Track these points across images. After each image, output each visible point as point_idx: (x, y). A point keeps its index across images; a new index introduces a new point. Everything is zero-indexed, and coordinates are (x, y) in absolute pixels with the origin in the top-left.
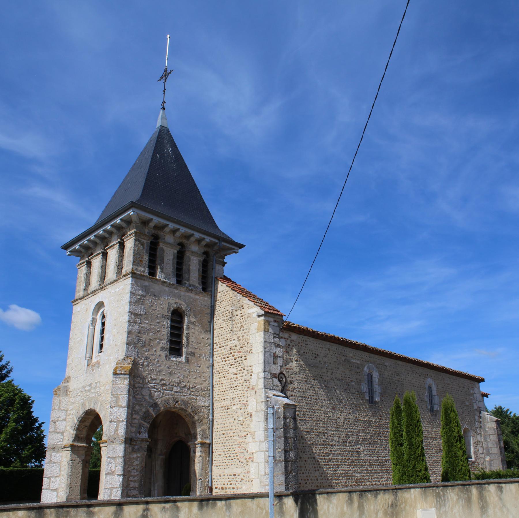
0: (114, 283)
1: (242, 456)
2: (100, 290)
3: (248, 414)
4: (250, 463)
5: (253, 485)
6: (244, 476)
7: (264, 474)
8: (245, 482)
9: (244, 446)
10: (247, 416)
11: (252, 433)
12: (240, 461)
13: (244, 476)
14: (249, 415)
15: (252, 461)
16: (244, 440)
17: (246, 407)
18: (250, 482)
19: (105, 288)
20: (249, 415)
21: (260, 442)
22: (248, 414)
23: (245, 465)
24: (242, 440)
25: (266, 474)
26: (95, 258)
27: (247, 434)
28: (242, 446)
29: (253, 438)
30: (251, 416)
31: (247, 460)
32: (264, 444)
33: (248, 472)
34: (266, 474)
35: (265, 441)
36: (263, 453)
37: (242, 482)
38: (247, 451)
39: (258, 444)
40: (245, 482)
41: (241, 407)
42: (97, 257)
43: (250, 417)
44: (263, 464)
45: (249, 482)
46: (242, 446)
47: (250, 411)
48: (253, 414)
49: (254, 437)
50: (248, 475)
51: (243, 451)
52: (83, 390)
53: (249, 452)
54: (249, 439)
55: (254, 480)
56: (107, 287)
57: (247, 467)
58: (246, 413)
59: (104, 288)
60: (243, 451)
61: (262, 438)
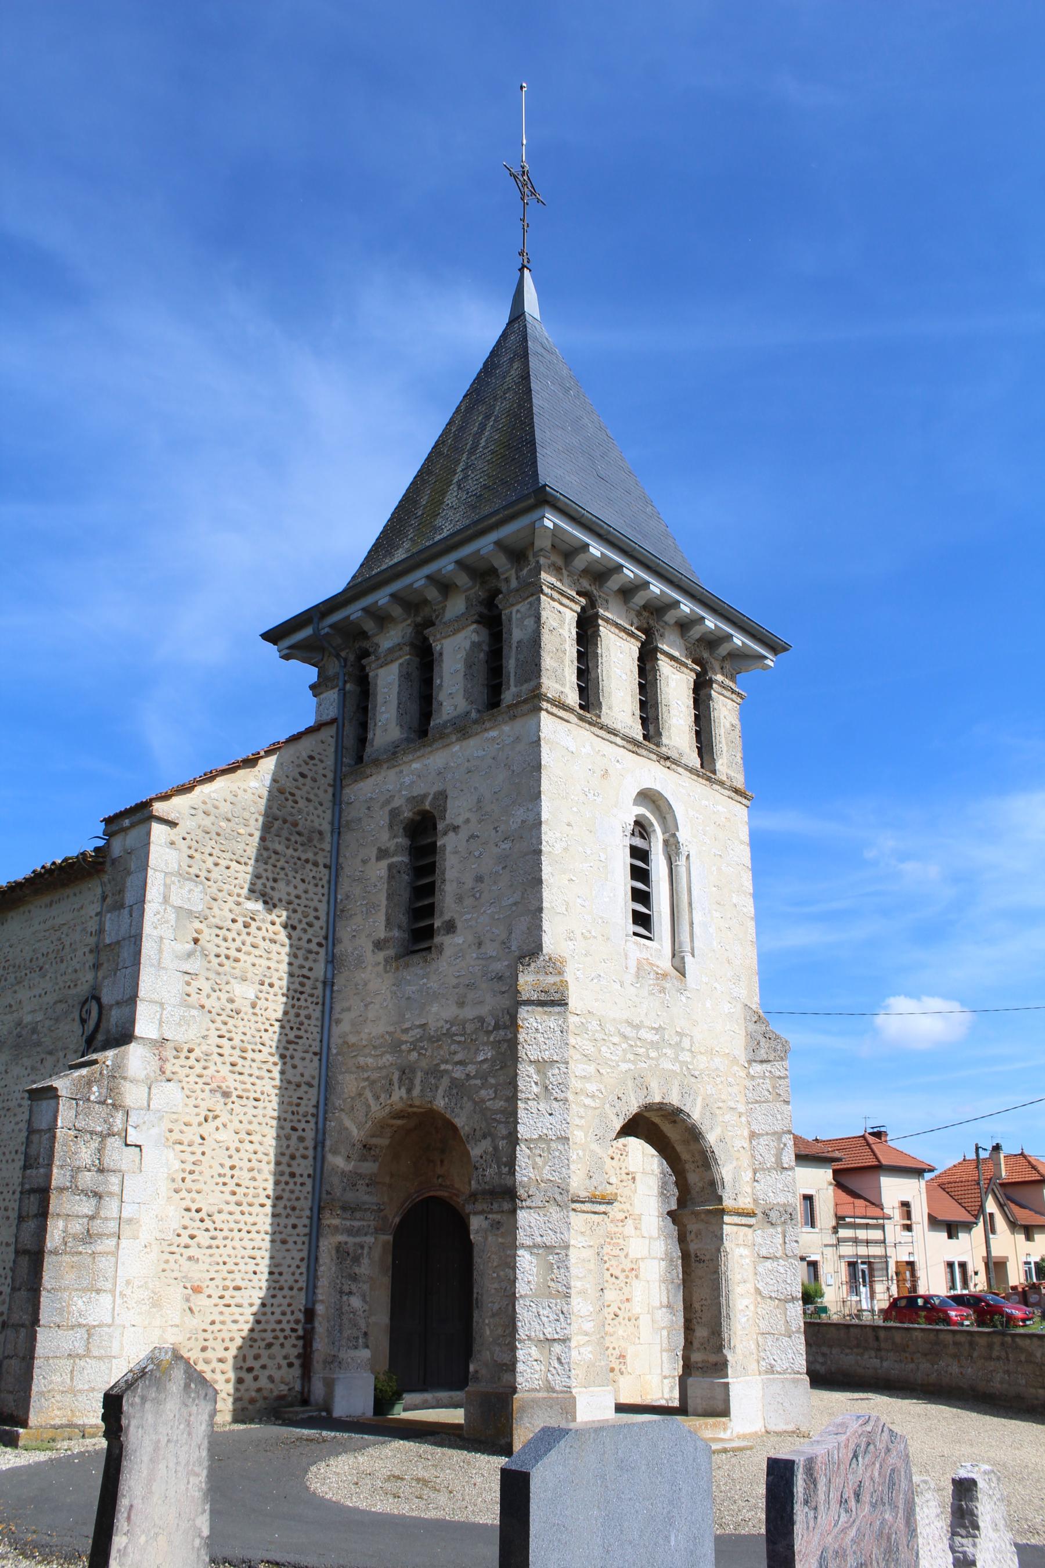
0: (700, 780)
1: (614, 1262)
2: (654, 757)
3: (628, 1174)
4: (635, 1282)
5: (641, 1327)
6: (620, 1309)
7: (658, 1305)
8: (622, 1321)
9: (621, 1241)
10: (625, 1177)
11: (636, 1217)
12: (612, 1275)
13: (620, 1309)
14: (630, 1177)
15: (637, 1277)
16: (620, 1229)
17: (624, 1156)
18: (633, 1320)
19: (673, 766)
20: (630, 1177)
21: (650, 1238)
22: (628, 1174)
23: (623, 1285)
24: (616, 1229)
25: (662, 1306)
26: (617, 631)
27: (626, 1218)
28: (615, 1241)
29: (636, 1228)
30: (634, 1178)
31: (627, 1273)
32: (657, 1243)
33: (628, 1300)
34: (662, 1306)
35: (659, 1237)
36: (656, 1262)
37: (615, 1322)
38: (626, 1256)
39: (647, 1241)
40: (622, 1321)
41: (614, 1155)
42: (622, 634)
43: (630, 1182)
44: (657, 1284)
45: (629, 1320)
46: (615, 1241)
47: (631, 1169)
48: (638, 1177)
49: (639, 1226)
50: (626, 1304)
51: (618, 1252)
52: (628, 1031)
53: (631, 1256)
54: (629, 1229)
55: (641, 1317)
56: (680, 770)
57: (626, 1290)
58: (624, 1171)
59: (668, 764)
60: (618, 1252)
61: (655, 1233)
